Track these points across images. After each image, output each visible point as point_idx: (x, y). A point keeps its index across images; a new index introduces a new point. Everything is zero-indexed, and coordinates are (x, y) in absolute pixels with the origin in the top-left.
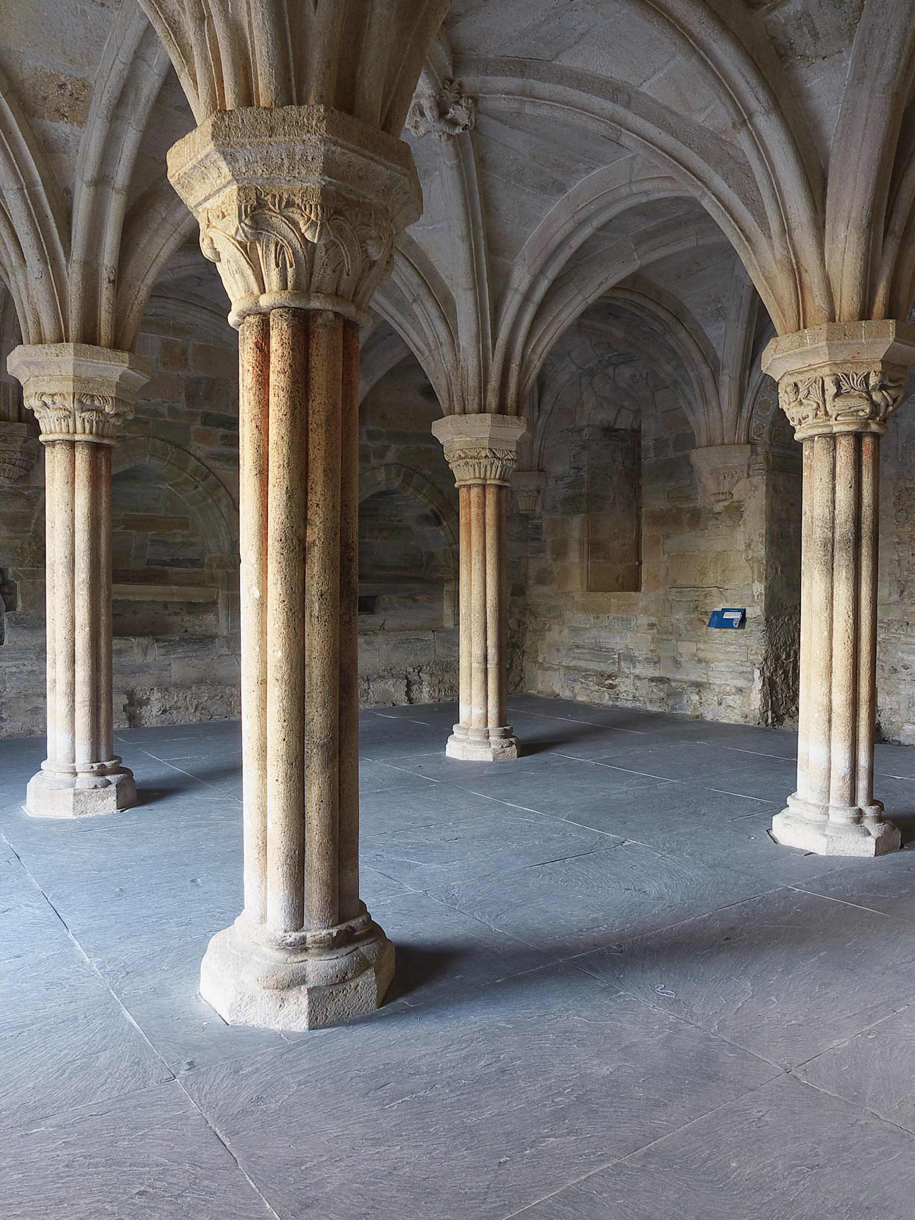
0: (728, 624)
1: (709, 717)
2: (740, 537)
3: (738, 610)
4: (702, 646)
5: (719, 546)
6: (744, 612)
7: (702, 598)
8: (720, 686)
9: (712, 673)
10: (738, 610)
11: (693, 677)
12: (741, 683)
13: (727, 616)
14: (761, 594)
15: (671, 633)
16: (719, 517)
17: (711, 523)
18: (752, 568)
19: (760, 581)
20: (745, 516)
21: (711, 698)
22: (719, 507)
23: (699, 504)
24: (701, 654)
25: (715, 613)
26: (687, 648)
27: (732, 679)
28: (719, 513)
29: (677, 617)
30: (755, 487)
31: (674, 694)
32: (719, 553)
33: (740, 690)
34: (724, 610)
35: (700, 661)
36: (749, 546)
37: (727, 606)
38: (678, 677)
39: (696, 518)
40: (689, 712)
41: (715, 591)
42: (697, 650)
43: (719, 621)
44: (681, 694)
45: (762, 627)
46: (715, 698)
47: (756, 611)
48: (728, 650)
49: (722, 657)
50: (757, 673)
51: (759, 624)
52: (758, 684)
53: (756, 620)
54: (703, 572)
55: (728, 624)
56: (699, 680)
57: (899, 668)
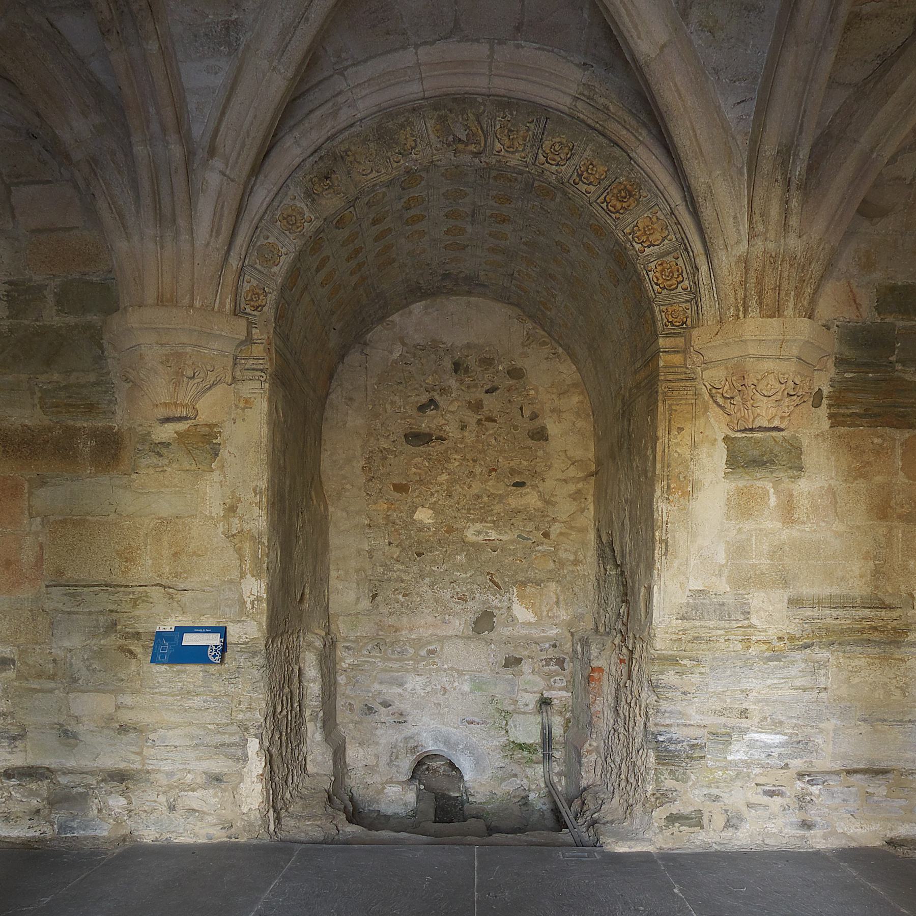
0: (199, 655)
1: (149, 835)
2: (212, 492)
3: (213, 630)
4: (128, 700)
5: (165, 505)
6: (223, 631)
7: (126, 607)
8: (170, 774)
9: (152, 751)
10: (213, 630)
11: (110, 761)
12: (218, 765)
13: (189, 640)
14: (259, 599)
15: (52, 677)
16: (164, 451)
17: (144, 462)
18: (239, 551)
19: (257, 576)
20: (224, 453)
21: (150, 799)
22: (167, 432)
23: (119, 421)
24: (126, 716)
25: (160, 636)
26: (91, 706)
27: (199, 759)
28: (167, 445)
29: (67, 644)
30: (247, 401)
31: (66, 799)
32: (165, 521)
33: (217, 779)
34: (181, 631)
35: (124, 729)
36: (232, 509)
37: (185, 621)
38: (71, 763)
39: (110, 450)
40: (104, 830)
41: (156, 593)
42: (118, 707)
43: (172, 650)
44: (84, 797)
45: (260, 660)
46: (162, 799)
47: (248, 630)
48: (188, 704)
49: (174, 718)
50: (253, 745)
51: (255, 654)
52: (256, 765)
53: (249, 649)
54: (128, 557)
55: (199, 655)
56: (122, 766)
57: (376, 706)
